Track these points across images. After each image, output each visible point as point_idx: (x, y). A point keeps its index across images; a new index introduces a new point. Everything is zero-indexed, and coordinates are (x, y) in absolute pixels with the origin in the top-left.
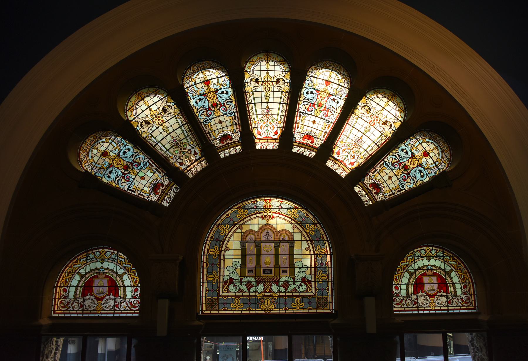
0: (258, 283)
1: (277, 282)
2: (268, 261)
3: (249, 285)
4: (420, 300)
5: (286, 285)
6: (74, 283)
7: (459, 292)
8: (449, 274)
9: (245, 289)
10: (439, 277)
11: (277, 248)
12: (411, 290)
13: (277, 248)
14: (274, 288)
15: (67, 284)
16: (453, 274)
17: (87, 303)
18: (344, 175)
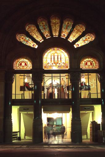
0: (54, 63)
1: (58, 63)
2: (56, 59)
3: (52, 64)
4: (87, 67)
5: (60, 64)
6: (18, 63)
7: (94, 65)
8: (93, 62)
9: (52, 64)
10: (91, 63)
11: (58, 57)
12: (85, 65)
13: (58, 57)
14: (57, 64)
15: (17, 64)
16: (93, 62)
17: (21, 67)
18: (71, 42)
